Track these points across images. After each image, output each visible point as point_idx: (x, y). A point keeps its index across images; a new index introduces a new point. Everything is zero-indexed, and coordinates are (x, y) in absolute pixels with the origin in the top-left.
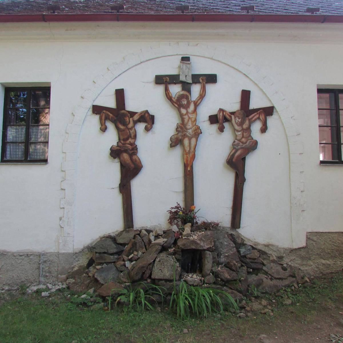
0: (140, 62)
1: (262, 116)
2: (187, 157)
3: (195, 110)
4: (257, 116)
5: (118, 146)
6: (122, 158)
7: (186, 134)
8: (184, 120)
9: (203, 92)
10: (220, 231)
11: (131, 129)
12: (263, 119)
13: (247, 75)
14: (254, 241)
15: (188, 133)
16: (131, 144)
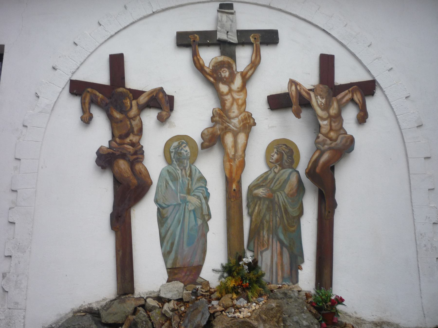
0: (152, 12)
1: (357, 95)
2: (231, 166)
3: (243, 88)
4: (349, 96)
5: (110, 147)
6: (116, 169)
7: (229, 126)
8: (225, 104)
10: (292, 300)
11: (134, 118)
12: (359, 100)
13: (327, 31)
14: (355, 315)
15: (233, 124)
16: (133, 144)
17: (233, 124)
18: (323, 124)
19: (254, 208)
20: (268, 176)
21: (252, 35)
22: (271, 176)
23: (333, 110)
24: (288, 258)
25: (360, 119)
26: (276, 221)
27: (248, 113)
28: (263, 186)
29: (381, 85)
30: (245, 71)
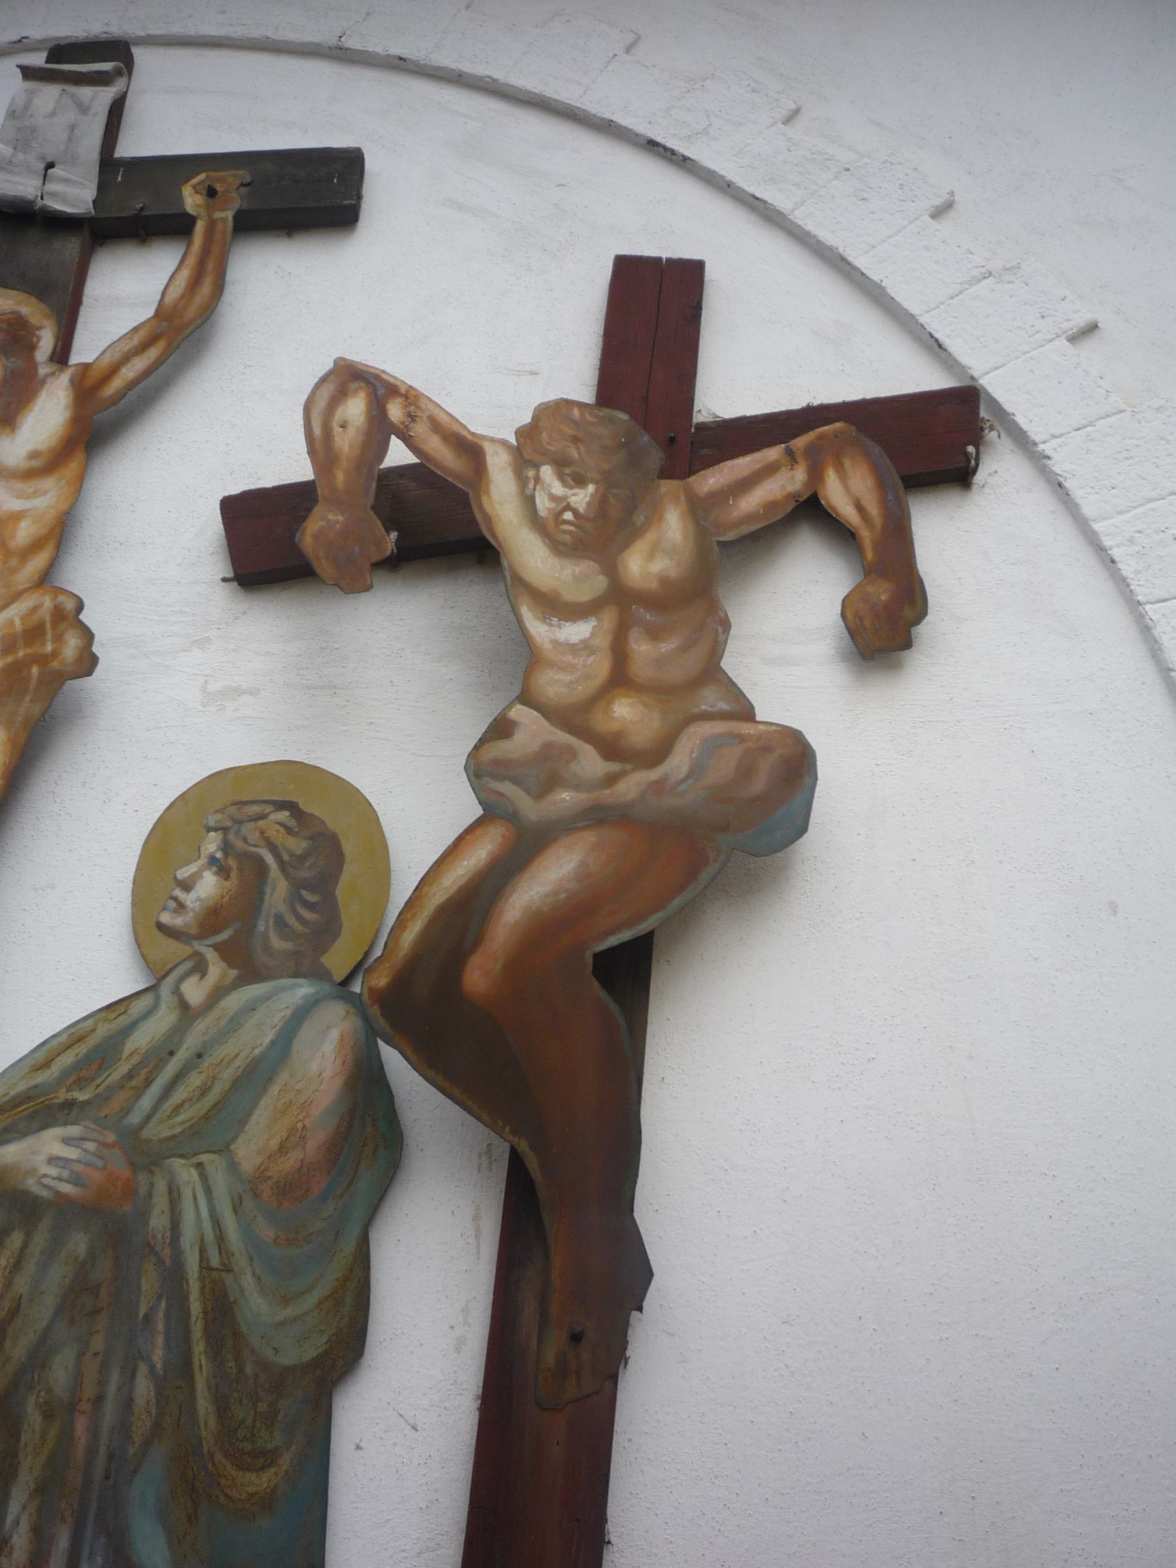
4: (791, 481)
9: (195, 282)
12: (860, 508)
18: (556, 643)
21: (202, 176)
22: (143, 1038)
23: (650, 556)
25: (867, 623)
26: (128, 1403)
27: (61, 598)
28: (75, 1111)
29: (1021, 420)
30: (107, 360)
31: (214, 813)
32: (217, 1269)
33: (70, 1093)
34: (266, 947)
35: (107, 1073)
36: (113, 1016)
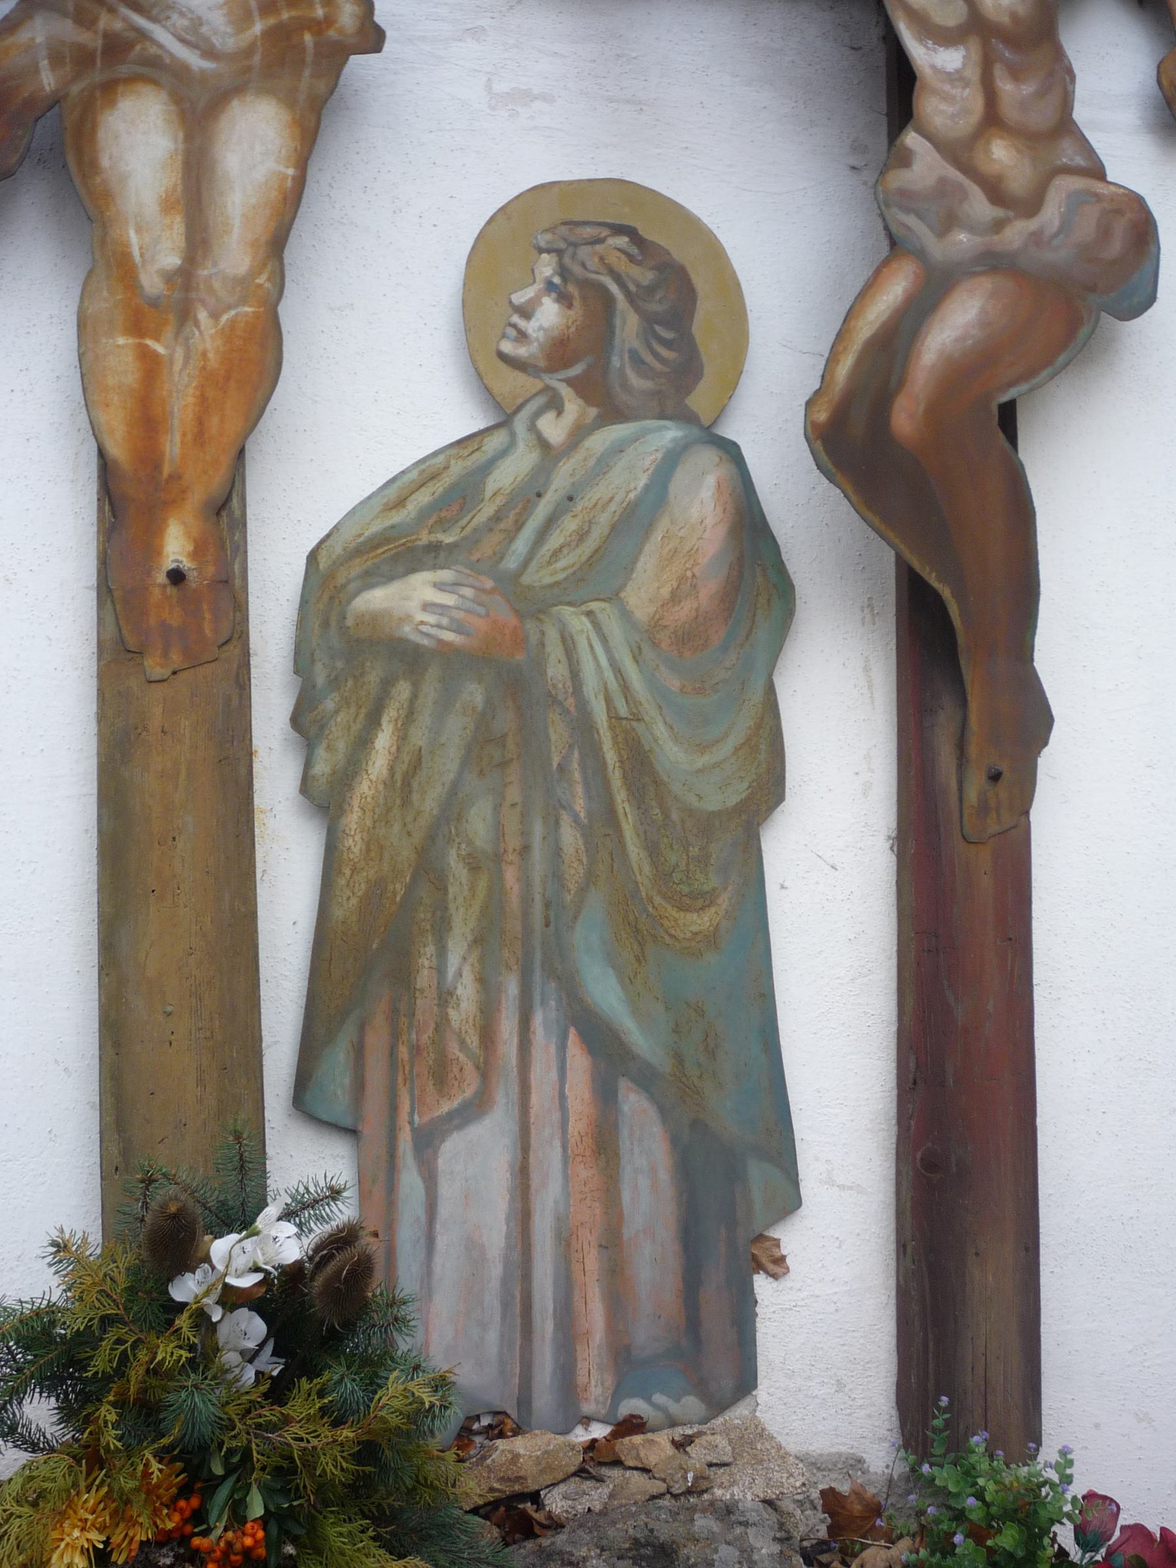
2: (151, 365)
7: (143, 35)
17: (181, 23)
18: (933, 67)
19: (363, 743)
20: (486, 468)
24: (664, 1176)
26: (557, 852)
28: (442, 555)
31: (543, 232)
32: (626, 719)
33: (432, 535)
34: (625, 386)
35: (471, 515)
36: (466, 452)
